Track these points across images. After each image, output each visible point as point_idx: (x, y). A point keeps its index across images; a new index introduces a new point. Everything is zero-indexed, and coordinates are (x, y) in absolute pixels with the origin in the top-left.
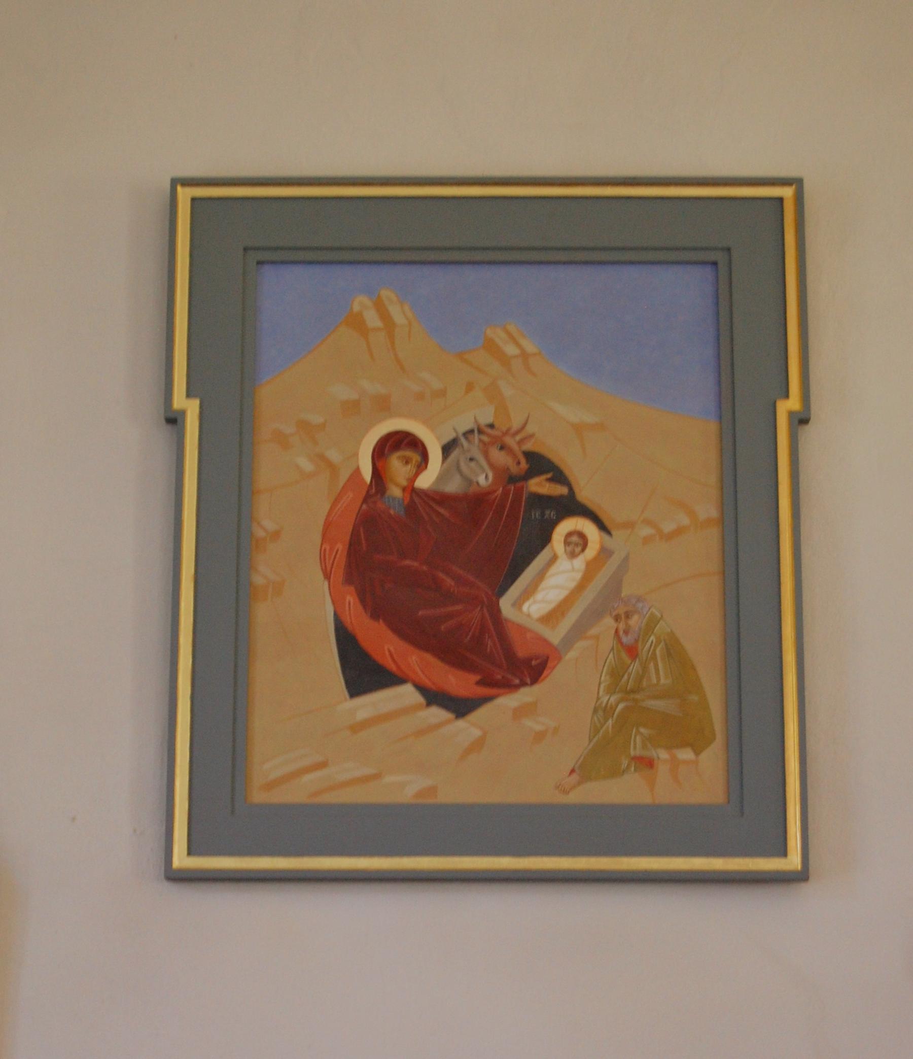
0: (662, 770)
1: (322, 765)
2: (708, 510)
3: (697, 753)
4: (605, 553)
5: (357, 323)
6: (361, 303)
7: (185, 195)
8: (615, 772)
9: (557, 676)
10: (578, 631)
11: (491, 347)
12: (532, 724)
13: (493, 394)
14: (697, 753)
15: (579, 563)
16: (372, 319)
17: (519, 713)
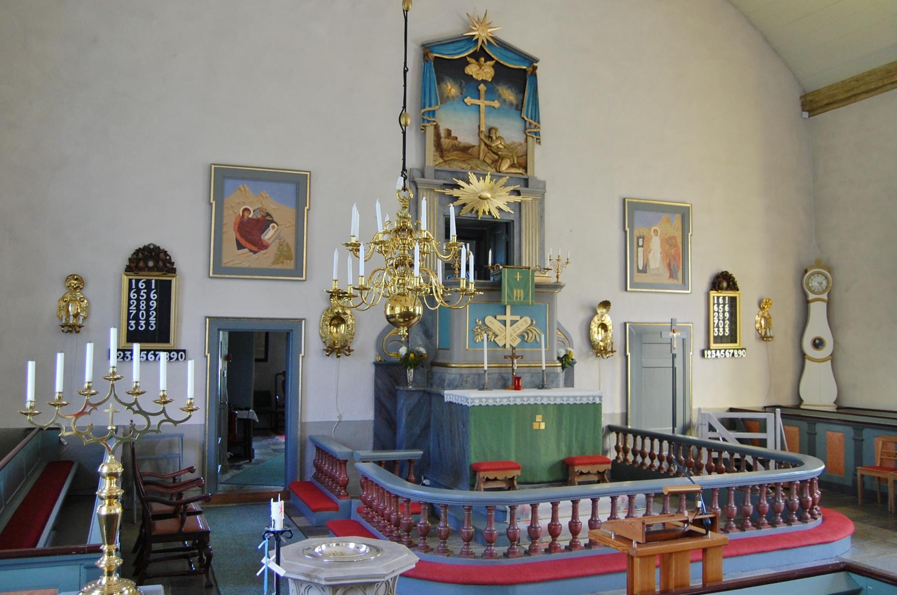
0: (285, 264)
1: (233, 261)
2: (294, 223)
3: (290, 261)
4: (278, 229)
5: (240, 190)
6: (241, 186)
7: (213, 166)
8: (278, 264)
9: (269, 248)
10: (273, 241)
11: (262, 196)
12: (265, 256)
13: (262, 203)
14: (290, 261)
15: (274, 231)
16: (243, 189)
17: (264, 254)
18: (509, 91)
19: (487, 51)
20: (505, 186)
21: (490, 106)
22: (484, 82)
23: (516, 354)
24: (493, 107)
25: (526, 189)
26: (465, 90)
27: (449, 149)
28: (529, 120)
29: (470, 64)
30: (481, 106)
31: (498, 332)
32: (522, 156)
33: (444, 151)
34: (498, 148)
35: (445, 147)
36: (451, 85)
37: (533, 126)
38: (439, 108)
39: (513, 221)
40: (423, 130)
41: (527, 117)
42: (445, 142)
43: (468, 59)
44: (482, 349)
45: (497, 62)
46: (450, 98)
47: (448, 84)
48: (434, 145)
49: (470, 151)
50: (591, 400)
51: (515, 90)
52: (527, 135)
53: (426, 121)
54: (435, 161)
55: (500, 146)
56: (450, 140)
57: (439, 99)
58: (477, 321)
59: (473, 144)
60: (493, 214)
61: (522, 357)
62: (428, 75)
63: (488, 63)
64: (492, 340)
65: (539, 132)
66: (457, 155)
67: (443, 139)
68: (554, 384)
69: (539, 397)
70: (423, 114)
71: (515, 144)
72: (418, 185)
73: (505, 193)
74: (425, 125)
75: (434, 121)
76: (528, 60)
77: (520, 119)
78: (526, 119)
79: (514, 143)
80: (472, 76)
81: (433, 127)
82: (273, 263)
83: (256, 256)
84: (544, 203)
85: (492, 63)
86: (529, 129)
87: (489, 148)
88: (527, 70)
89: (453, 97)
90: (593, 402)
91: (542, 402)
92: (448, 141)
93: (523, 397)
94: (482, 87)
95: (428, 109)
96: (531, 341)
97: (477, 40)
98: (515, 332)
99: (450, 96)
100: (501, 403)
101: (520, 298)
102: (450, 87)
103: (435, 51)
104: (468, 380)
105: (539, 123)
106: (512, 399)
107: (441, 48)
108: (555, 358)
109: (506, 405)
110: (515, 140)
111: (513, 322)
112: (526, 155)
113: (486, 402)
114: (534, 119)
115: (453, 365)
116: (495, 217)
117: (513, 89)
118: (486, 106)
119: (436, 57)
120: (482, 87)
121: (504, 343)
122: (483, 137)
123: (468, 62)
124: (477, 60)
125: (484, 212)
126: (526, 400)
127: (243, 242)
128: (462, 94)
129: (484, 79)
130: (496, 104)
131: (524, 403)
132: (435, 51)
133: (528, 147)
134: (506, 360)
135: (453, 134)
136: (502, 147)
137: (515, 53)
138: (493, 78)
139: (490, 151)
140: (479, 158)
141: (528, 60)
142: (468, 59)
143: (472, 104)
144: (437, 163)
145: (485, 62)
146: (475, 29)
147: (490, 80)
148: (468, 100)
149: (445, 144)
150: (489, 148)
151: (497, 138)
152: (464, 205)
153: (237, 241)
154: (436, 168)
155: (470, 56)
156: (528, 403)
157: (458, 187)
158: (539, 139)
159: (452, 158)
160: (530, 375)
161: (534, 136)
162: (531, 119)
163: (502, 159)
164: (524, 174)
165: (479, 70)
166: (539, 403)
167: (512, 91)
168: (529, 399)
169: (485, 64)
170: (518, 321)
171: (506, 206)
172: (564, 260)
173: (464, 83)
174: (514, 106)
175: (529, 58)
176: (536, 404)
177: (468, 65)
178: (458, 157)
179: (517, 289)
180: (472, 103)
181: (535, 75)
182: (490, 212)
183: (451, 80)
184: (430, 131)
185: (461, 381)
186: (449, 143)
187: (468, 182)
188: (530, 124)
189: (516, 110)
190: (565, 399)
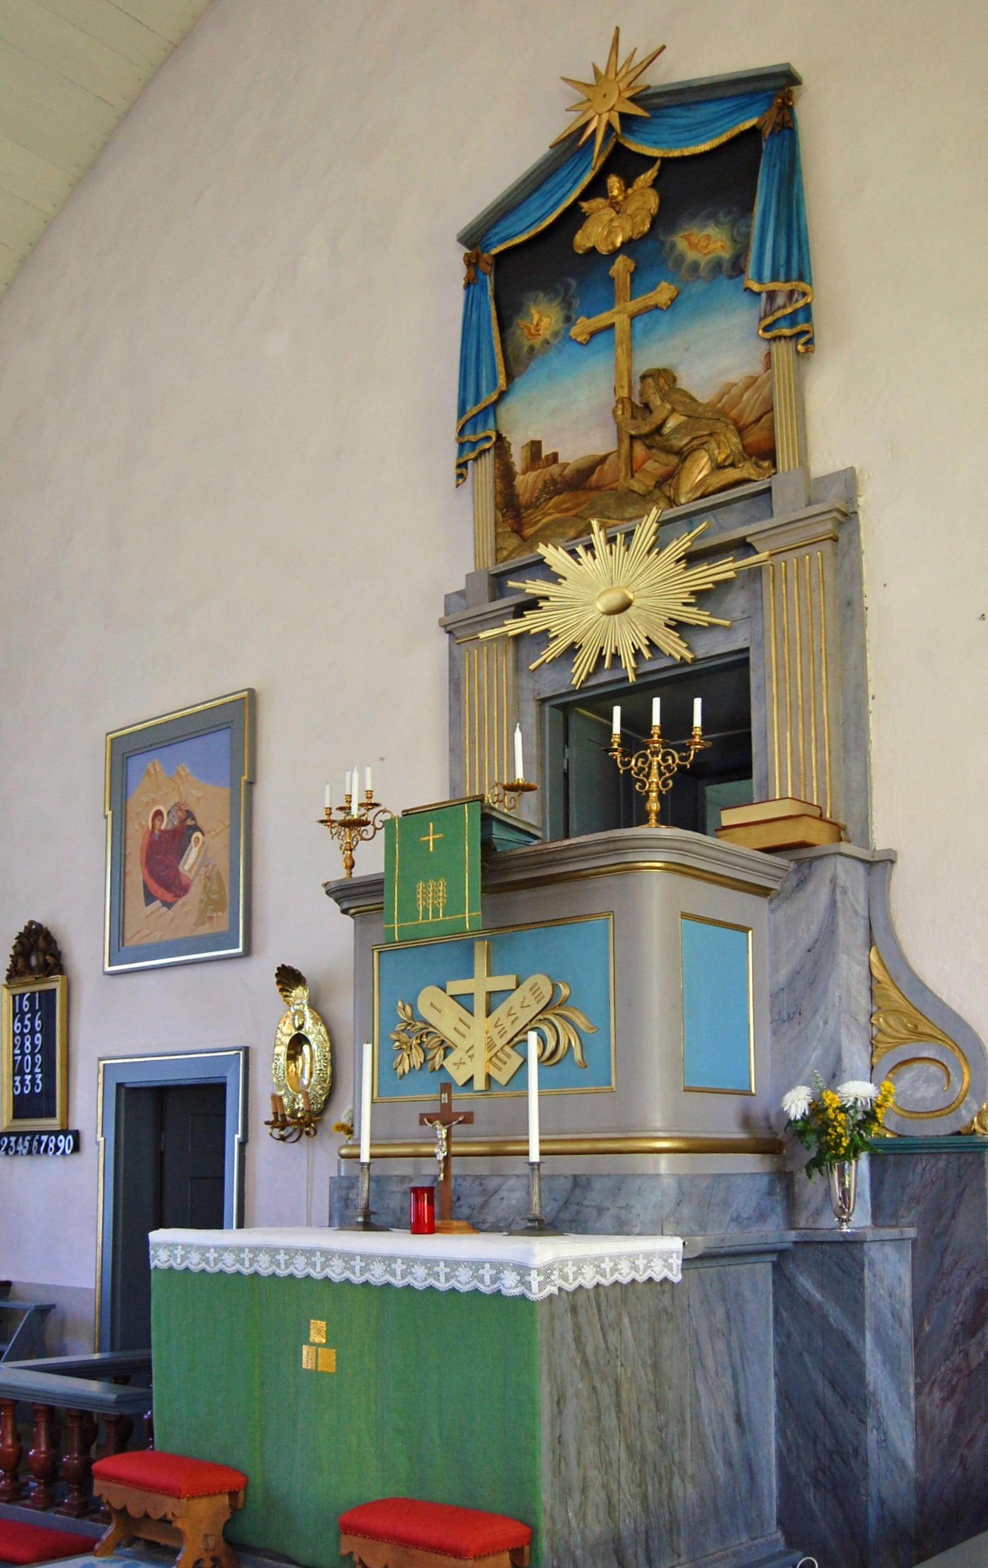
0: (215, 919)
1: (139, 932)
2: (227, 822)
3: (223, 912)
4: (203, 843)
5: (148, 773)
11: (179, 774)
12: (185, 909)
14: (223, 912)
15: (197, 849)
16: (152, 771)
17: (183, 905)
20: (659, 544)
24: (656, 307)
27: (538, 499)
31: (451, 1036)
32: (758, 420)
38: (502, 395)
41: (760, 280)
42: (525, 482)
43: (585, 205)
45: (666, 161)
48: (496, 506)
50: (487, 1280)
51: (728, 213)
60: (667, 649)
66: (557, 508)
67: (522, 477)
73: (673, 565)
82: (197, 924)
83: (170, 913)
99: (537, 342)
102: (536, 317)
107: (505, 224)
111: (494, 999)
117: (721, 217)
126: (398, 1272)
127: (155, 888)
135: (546, 451)
143: (593, 334)
149: (526, 489)
152: (572, 650)
153: (145, 886)
159: (546, 520)
164: (756, 479)
169: (630, 191)
170: (513, 990)
171: (694, 610)
173: (573, 283)
174: (726, 267)
175: (759, 85)
178: (561, 512)
179: (426, 882)
180: (592, 329)
182: (652, 646)
184: (485, 468)
186: (535, 482)
187: (554, 578)
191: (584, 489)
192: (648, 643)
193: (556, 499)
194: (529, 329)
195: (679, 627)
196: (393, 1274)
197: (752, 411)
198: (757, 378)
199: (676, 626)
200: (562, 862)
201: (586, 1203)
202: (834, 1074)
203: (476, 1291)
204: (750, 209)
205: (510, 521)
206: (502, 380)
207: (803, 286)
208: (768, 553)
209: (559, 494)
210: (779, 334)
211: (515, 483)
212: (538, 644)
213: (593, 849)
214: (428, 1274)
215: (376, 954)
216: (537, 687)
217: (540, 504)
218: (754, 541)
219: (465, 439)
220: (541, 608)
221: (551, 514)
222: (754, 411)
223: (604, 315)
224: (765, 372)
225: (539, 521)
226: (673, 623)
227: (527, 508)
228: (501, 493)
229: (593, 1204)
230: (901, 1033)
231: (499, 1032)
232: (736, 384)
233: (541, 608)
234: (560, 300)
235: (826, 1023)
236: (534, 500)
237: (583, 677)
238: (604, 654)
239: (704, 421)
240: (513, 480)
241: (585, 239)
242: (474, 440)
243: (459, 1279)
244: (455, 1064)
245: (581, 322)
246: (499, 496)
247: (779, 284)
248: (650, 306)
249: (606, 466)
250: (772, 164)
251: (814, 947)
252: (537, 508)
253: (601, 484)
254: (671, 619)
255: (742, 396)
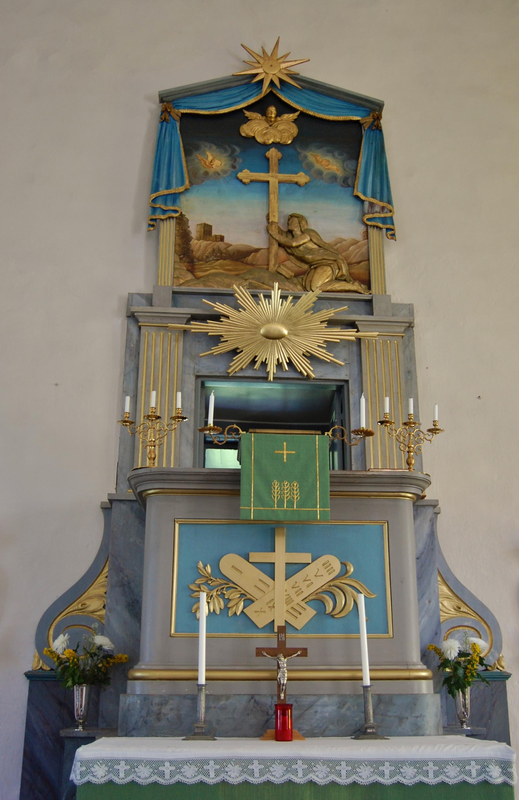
18: (329, 158)
19: (283, 99)
20: (315, 308)
21: (290, 183)
22: (275, 144)
23: (288, 645)
24: (296, 183)
25: (370, 318)
26: (240, 160)
27: (207, 257)
28: (368, 199)
29: (250, 120)
30: (270, 183)
31: (254, 593)
32: (359, 262)
33: (195, 260)
34: (307, 248)
35: (197, 254)
36: (212, 155)
37: (377, 209)
38: (187, 190)
39: (347, 381)
40: (153, 226)
41: (365, 194)
43: (247, 114)
44: (207, 634)
45: (303, 114)
46: (210, 174)
47: (208, 153)
48: (175, 251)
49: (250, 258)
50: (474, 773)
51: (341, 154)
52: (367, 225)
53: (158, 211)
54: (176, 278)
55: (311, 245)
56: (209, 242)
57: (186, 175)
58: (201, 565)
59: (256, 246)
61: (304, 652)
62: (167, 140)
63: (286, 116)
64: (238, 614)
65: (391, 218)
66: (222, 266)
67: (196, 241)
68: (407, 725)
69: (300, 762)
70: (154, 201)
71: (344, 243)
72: (140, 319)
73: (319, 323)
74: (157, 217)
75: (176, 211)
76: (364, 106)
77: (352, 200)
78: (362, 197)
79: (341, 240)
80: (254, 137)
81: (173, 223)
84: (413, 345)
85: (293, 116)
86: (368, 213)
87: (289, 251)
88: (361, 122)
89: (217, 173)
90: (481, 778)
91: (312, 777)
92: (204, 243)
93: (250, 761)
94: (273, 153)
95: (163, 191)
96: (343, 614)
97: (261, 82)
98: (298, 594)
99: (211, 171)
100: (178, 778)
101: (290, 503)
102: (210, 158)
103: (183, 105)
104: (165, 710)
105: (390, 202)
106: (212, 768)
108: (415, 656)
109: (282, 785)
110: (344, 236)
112: (369, 260)
113: (127, 773)
114: (378, 196)
115: (138, 674)
116: (305, 374)
117: (336, 154)
118: (279, 182)
119: (183, 114)
120: (273, 153)
121: (273, 620)
122: (274, 232)
123: (247, 117)
124: (264, 113)
125: (279, 365)
128: (234, 167)
129: (278, 140)
130: (302, 178)
131: (251, 779)
132: (183, 105)
133: (371, 245)
134: (260, 658)
135: (215, 232)
136: (315, 247)
137: (337, 98)
138: (295, 140)
139: (292, 257)
140: (268, 269)
141: (364, 106)
142: (247, 114)
143: (252, 181)
144: (182, 281)
145: (279, 114)
146: (257, 65)
147: (289, 142)
148: (245, 175)
149: (199, 250)
150: (289, 251)
151: (302, 232)
152: (235, 352)
154: (176, 289)
155: (249, 108)
156: (264, 779)
157: (217, 317)
158: (393, 230)
160: (335, 699)
161: (381, 225)
162: (374, 196)
163: (315, 268)
164: (363, 292)
165: (267, 128)
166: (299, 779)
167: (334, 156)
168: (354, 768)
169: (279, 119)
170: (309, 564)
171: (324, 351)
172: (426, 425)
173: (238, 150)
175: (364, 103)
176: (290, 782)
177: (245, 123)
178: (225, 270)
179: (281, 482)
180: (253, 178)
181: (379, 129)
182: (290, 364)
183: (214, 147)
185: (144, 713)
186: (206, 247)
187: (237, 307)
188: (372, 205)
189: (342, 186)
190: (387, 769)
191: (242, 262)
192: (288, 361)
193: (221, 261)
194: (205, 163)
195: (311, 358)
196: (382, 774)
197: (355, 257)
198: (359, 242)
199: (309, 356)
200: (360, 484)
201: (389, 714)
202: (436, 632)
203: (465, 782)
204: (357, 158)
205: (186, 263)
206: (187, 182)
207: (389, 207)
208: (378, 333)
209: (224, 259)
210: (377, 225)
211: (191, 243)
212: (199, 342)
213: (385, 480)
214: (418, 773)
215: (177, 525)
216: (197, 367)
217: (209, 261)
218: (360, 324)
219: (158, 206)
220: (222, 321)
221: (216, 269)
222: (356, 257)
223: (262, 174)
224: (363, 240)
225: (208, 270)
226: (309, 355)
227: (199, 260)
228: (179, 245)
229: (394, 714)
230: (451, 611)
231: (296, 592)
232: (345, 240)
233: (222, 321)
234: (228, 155)
235: (430, 602)
236: (204, 257)
237: (237, 370)
238: (256, 360)
239: (328, 252)
240: (190, 241)
241: (246, 130)
242: (165, 209)
243: (447, 774)
244: (256, 612)
245: (246, 172)
246: (177, 246)
247: (376, 201)
248: (293, 181)
249: (258, 255)
250: (371, 142)
251: (421, 557)
252: (207, 262)
253: (254, 263)
254: (307, 352)
255: (349, 247)
